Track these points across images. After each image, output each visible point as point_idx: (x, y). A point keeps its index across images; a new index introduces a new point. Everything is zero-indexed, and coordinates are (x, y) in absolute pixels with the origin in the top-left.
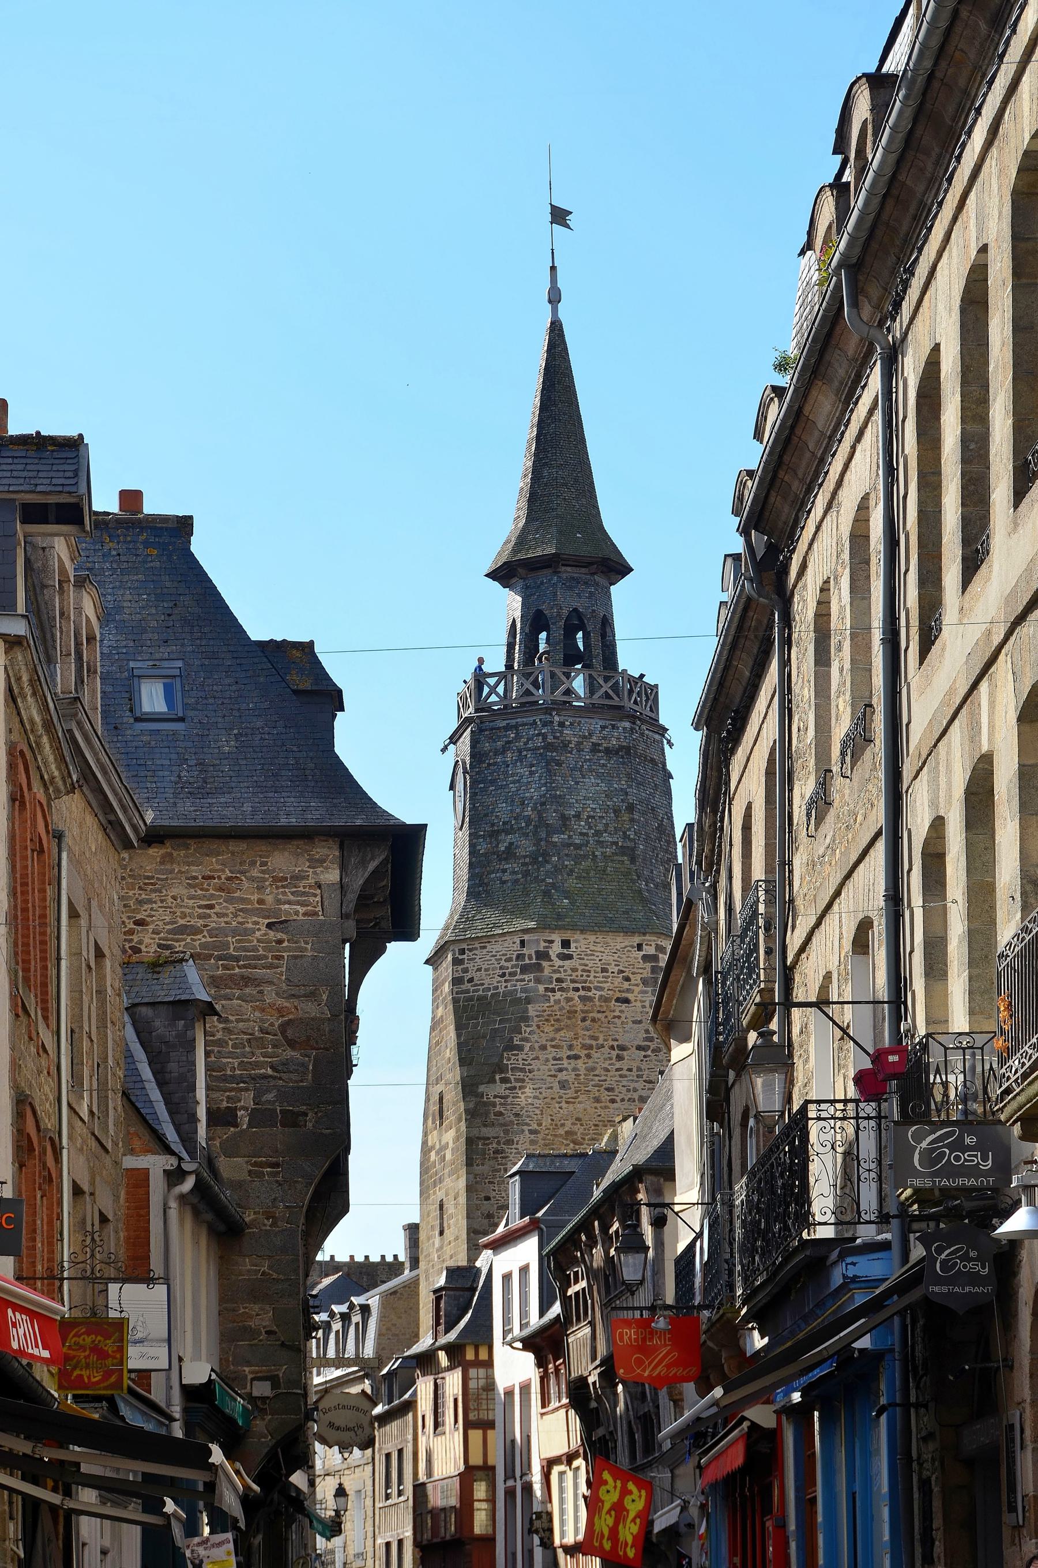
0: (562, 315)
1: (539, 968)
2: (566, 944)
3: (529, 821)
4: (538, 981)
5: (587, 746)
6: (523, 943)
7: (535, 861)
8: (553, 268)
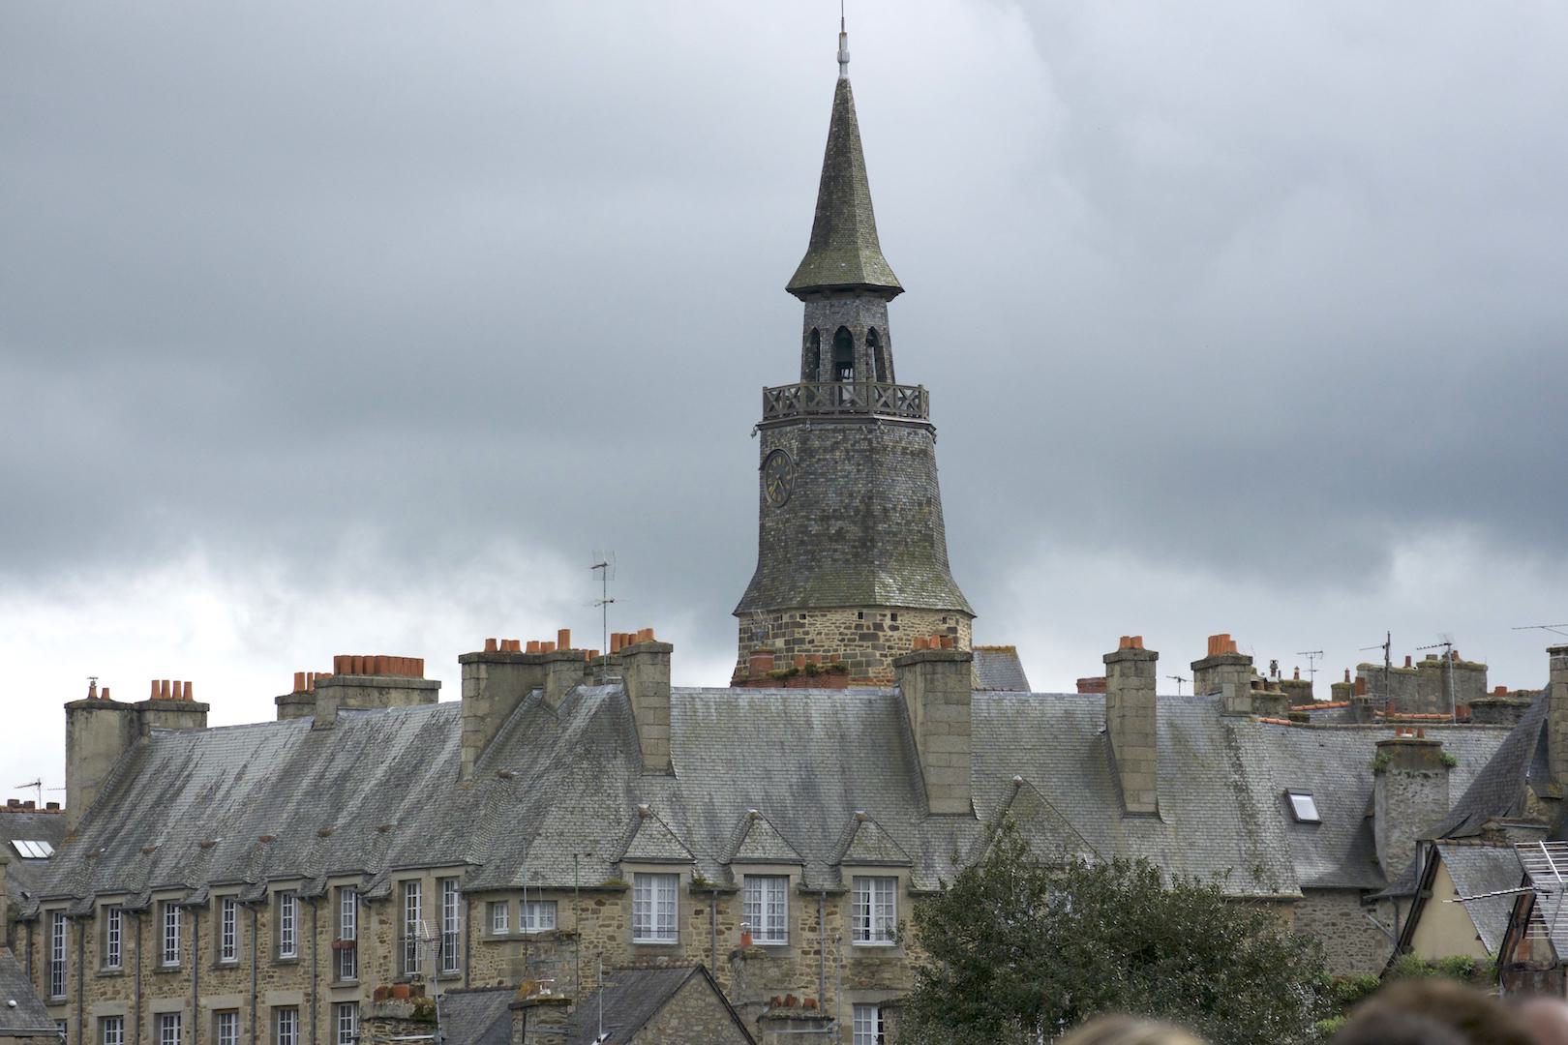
0: (853, 75)
1: (875, 637)
2: (894, 617)
3: (857, 511)
4: (875, 647)
5: (899, 450)
6: (861, 616)
7: (864, 545)
8: (843, 34)
